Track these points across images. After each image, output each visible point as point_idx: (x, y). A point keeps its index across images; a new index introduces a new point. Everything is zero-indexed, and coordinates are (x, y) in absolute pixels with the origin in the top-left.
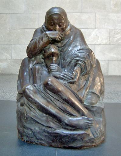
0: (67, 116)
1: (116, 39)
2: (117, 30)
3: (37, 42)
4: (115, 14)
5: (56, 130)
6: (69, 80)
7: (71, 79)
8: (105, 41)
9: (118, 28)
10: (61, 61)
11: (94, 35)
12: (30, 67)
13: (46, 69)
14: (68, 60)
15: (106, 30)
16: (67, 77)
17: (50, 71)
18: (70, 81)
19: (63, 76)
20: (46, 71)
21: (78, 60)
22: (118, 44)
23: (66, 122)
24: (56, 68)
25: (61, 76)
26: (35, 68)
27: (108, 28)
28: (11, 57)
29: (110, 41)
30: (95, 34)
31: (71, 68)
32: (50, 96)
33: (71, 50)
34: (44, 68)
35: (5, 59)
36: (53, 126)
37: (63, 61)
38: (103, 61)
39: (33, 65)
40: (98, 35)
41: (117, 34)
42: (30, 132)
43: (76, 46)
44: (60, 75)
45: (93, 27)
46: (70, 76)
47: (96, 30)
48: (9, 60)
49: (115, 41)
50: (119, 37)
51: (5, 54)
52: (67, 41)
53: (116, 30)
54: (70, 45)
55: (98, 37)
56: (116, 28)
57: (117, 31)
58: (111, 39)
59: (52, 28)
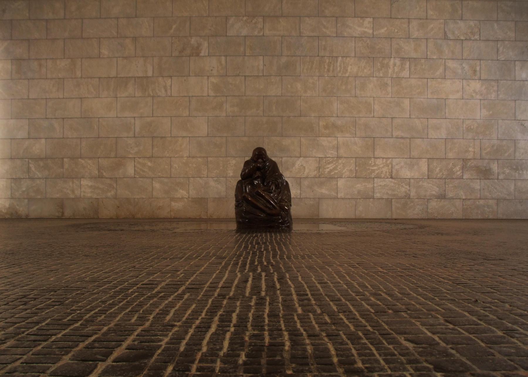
1: (328, 170)
2: (329, 159)
4: (325, 138)
8: (314, 173)
9: (330, 156)
11: (300, 165)
15: (314, 158)
22: (330, 177)
27: (317, 156)
28: (188, 195)
29: (320, 173)
30: (301, 164)
35: (180, 197)
38: (312, 199)
40: (304, 165)
41: (329, 163)
45: (298, 155)
47: (302, 158)
48: (185, 200)
49: (326, 173)
50: (331, 168)
51: (181, 191)
53: (327, 159)
55: (304, 167)
56: (328, 156)
57: (329, 160)
58: (321, 170)
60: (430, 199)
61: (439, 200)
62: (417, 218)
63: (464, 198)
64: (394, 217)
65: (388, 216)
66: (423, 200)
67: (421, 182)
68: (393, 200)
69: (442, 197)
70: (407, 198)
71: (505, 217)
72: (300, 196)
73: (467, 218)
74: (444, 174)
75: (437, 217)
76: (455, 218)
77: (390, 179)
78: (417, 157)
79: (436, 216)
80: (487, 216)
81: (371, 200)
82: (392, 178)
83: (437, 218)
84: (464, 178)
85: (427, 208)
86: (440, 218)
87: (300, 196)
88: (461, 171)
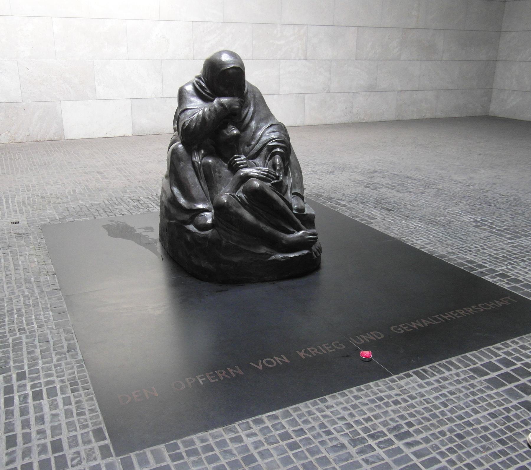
0: (282, 235)
3: (207, 117)
5: (272, 257)
6: (272, 180)
7: (275, 178)
10: (244, 148)
12: (198, 163)
13: (226, 164)
14: (259, 146)
16: (270, 175)
17: (234, 169)
18: (275, 181)
19: (263, 174)
20: (224, 166)
21: (275, 147)
23: (284, 242)
24: (245, 161)
25: (262, 176)
26: (208, 165)
31: (266, 158)
32: (258, 209)
33: (258, 129)
34: (220, 162)
36: (267, 251)
37: (246, 147)
39: (201, 158)
42: (231, 267)
43: (261, 120)
44: (258, 173)
46: (273, 173)
52: (246, 112)
54: (251, 119)
59: (227, 92)
60: (357, 92)
61: (368, 93)
62: (338, 123)
63: (399, 89)
64: (307, 123)
65: (299, 123)
66: (347, 94)
67: (346, 65)
68: (307, 96)
69: (371, 89)
70: (325, 92)
71: (443, 116)
72: (163, 95)
73: (400, 119)
74: (377, 52)
75: (363, 119)
76: (386, 119)
77: (304, 62)
78: (342, 25)
79: (362, 118)
80: (423, 115)
81: (276, 96)
82: (306, 59)
83: (364, 121)
84: (402, 58)
85: (352, 107)
86: (367, 121)
87: (163, 95)
88: (399, 48)
